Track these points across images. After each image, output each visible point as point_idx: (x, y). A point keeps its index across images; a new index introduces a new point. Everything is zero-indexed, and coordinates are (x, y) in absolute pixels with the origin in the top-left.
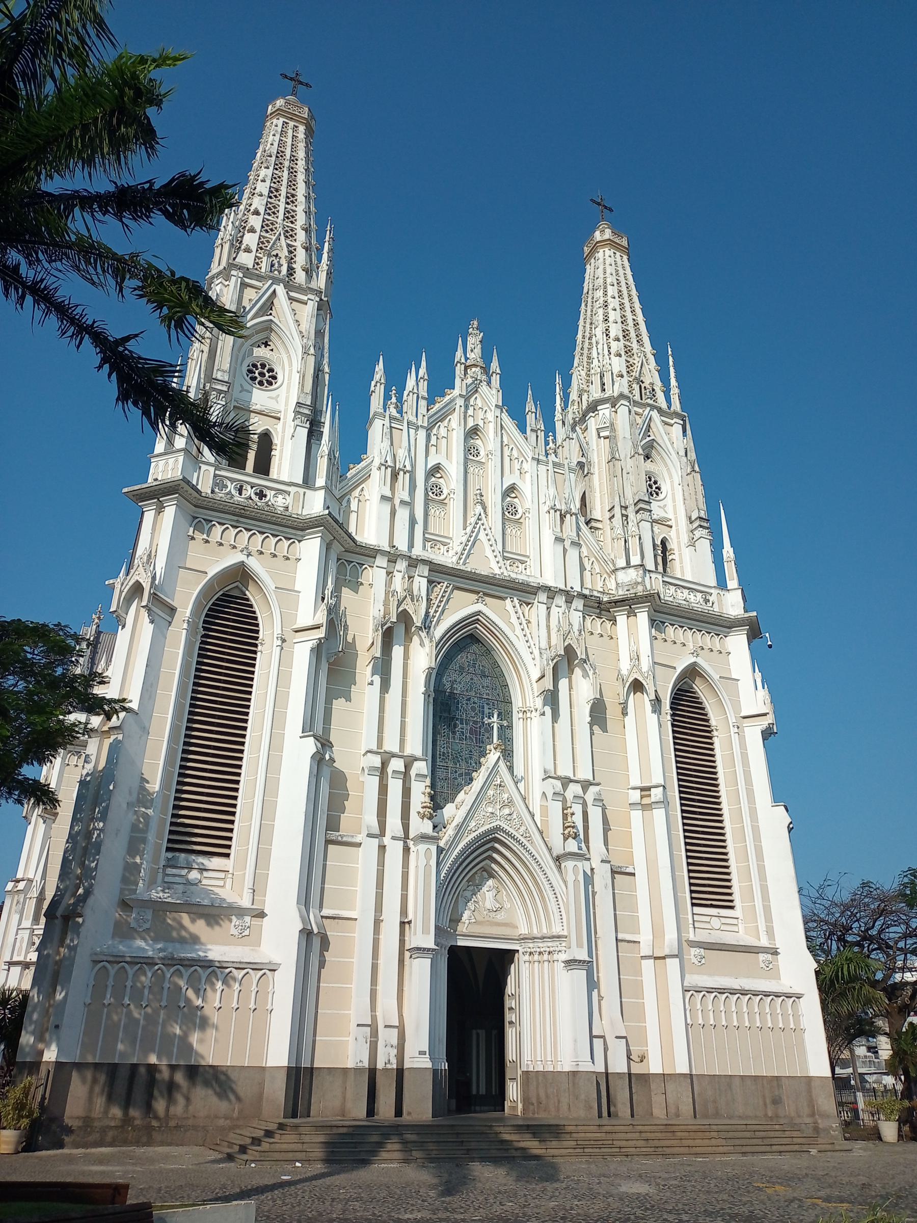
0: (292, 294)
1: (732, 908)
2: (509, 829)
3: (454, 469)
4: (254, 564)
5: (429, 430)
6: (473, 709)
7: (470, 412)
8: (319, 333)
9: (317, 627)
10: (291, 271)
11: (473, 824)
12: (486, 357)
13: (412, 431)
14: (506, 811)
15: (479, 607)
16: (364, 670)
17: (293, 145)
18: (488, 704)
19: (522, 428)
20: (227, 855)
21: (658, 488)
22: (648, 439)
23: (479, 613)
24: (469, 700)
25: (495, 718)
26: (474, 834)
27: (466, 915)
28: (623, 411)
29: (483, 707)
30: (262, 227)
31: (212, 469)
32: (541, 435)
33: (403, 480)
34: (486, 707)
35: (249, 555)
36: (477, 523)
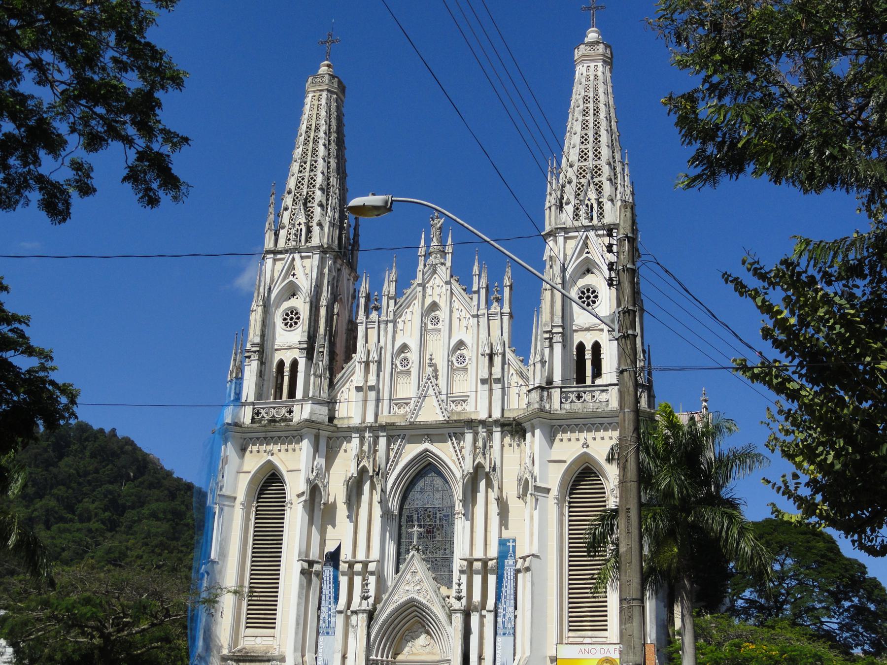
0: (303, 254)
1: (606, 630)
2: (418, 598)
3: (414, 344)
4: (275, 460)
5: (394, 322)
6: (429, 516)
7: (429, 291)
8: (321, 274)
9: (303, 493)
10: (309, 230)
11: (396, 597)
12: (443, 243)
13: (382, 326)
14: (418, 587)
15: (427, 445)
16: (342, 511)
17: (318, 114)
18: (439, 511)
19: (468, 290)
20: (274, 628)
21: (596, 297)
22: (585, 255)
23: (426, 450)
24: (426, 510)
25: (415, 529)
26: (396, 605)
27: (406, 649)
28: (561, 240)
29: (436, 514)
30: (294, 200)
31: (252, 407)
32: (483, 292)
33: (373, 367)
34: (438, 513)
35: (272, 454)
36: (426, 383)
